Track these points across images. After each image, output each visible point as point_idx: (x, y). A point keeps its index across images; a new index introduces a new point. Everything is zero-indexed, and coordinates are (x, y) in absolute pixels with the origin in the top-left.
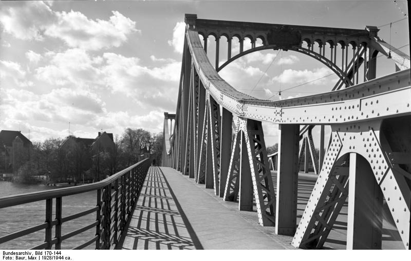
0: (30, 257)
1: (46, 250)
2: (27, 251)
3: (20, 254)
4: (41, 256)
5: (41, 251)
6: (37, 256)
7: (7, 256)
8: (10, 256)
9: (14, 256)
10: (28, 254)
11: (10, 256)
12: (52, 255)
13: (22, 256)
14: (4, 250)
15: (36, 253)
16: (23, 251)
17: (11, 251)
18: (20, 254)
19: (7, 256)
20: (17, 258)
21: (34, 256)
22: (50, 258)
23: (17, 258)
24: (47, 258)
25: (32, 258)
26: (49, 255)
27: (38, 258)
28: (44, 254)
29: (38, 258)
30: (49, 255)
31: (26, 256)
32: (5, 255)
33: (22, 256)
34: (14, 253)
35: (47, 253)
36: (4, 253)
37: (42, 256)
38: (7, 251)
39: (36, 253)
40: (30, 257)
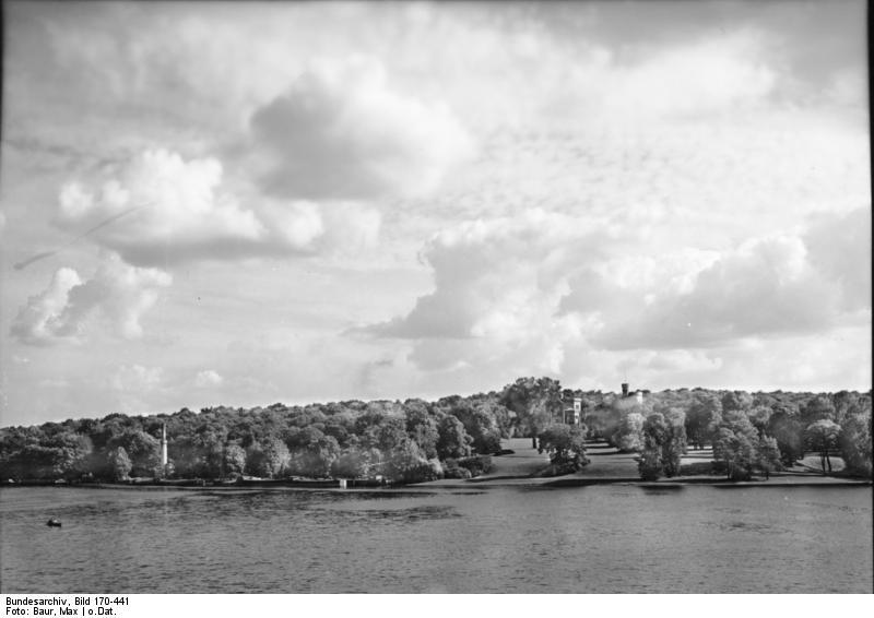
0: (64, 609)
2: (57, 596)
3: (43, 603)
4: (87, 608)
5: (86, 596)
6: (80, 608)
7: (15, 607)
8: (21, 607)
9: (30, 608)
10: (59, 603)
11: (21, 607)
13: (46, 607)
14: (8, 595)
15: (77, 602)
16: (50, 597)
17: (22, 597)
18: (43, 603)
19: (15, 607)
20: (36, 612)
21: (73, 607)
23: (36, 612)
25: (69, 612)
27: (80, 612)
28: (93, 602)
29: (80, 612)
31: (56, 608)
32: (11, 605)
33: (46, 607)
34: (30, 602)
35: (99, 600)
36: (8, 601)
38: (14, 597)
39: (77, 602)
40: (64, 609)
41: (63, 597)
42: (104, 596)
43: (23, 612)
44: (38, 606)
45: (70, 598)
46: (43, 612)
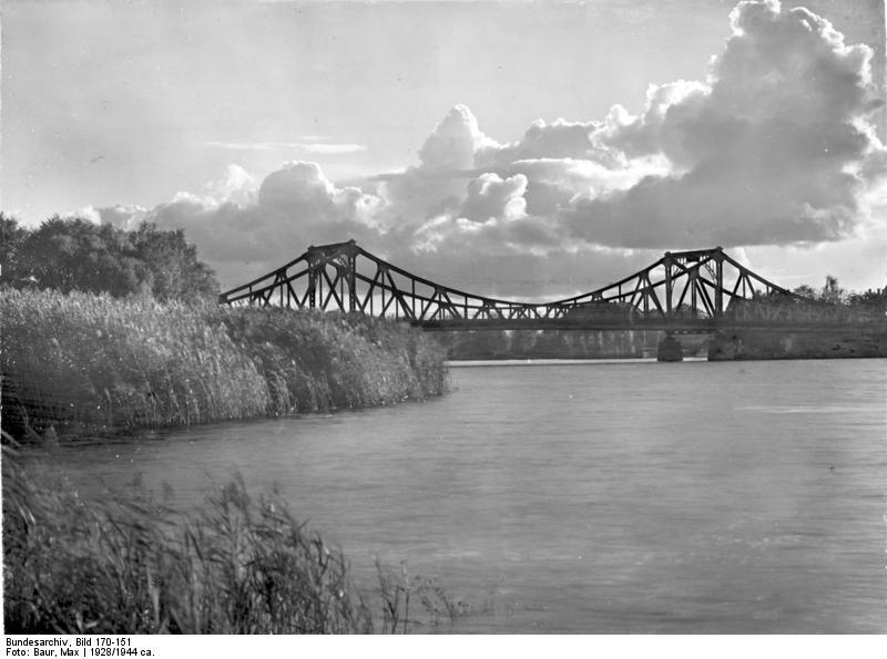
1: (100, 636)
2: (57, 637)
3: (43, 643)
4: (88, 648)
5: (88, 637)
6: (81, 648)
7: (15, 648)
8: (21, 648)
9: (31, 649)
10: (59, 643)
11: (21, 648)
12: (112, 647)
13: (47, 648)
15: (78, 642)
17: (23, 637)
18: (43, 643)
19: (15, 648)
20: (36, 653)
21: (74, 648)
22: (109, 653)
23: (36, 653)
24: (101, 652)
25: (70, 653)
26: (105, 646)
27: (81, 653)
28: (94, 642)
29: (81, 653)
30: (105, 646)
31: (57, 649)
33: (47, 648)
34: (31, 643)
35: (101, 642)
36: (9, 642)
37: (91, 647)
38: (14, 637)
39: (78, 642)
41: (64, 637)
42: (106, 636)
43: (24, 653)
44: (39, 647)
45: (71, 639)
46: (43, 653)
